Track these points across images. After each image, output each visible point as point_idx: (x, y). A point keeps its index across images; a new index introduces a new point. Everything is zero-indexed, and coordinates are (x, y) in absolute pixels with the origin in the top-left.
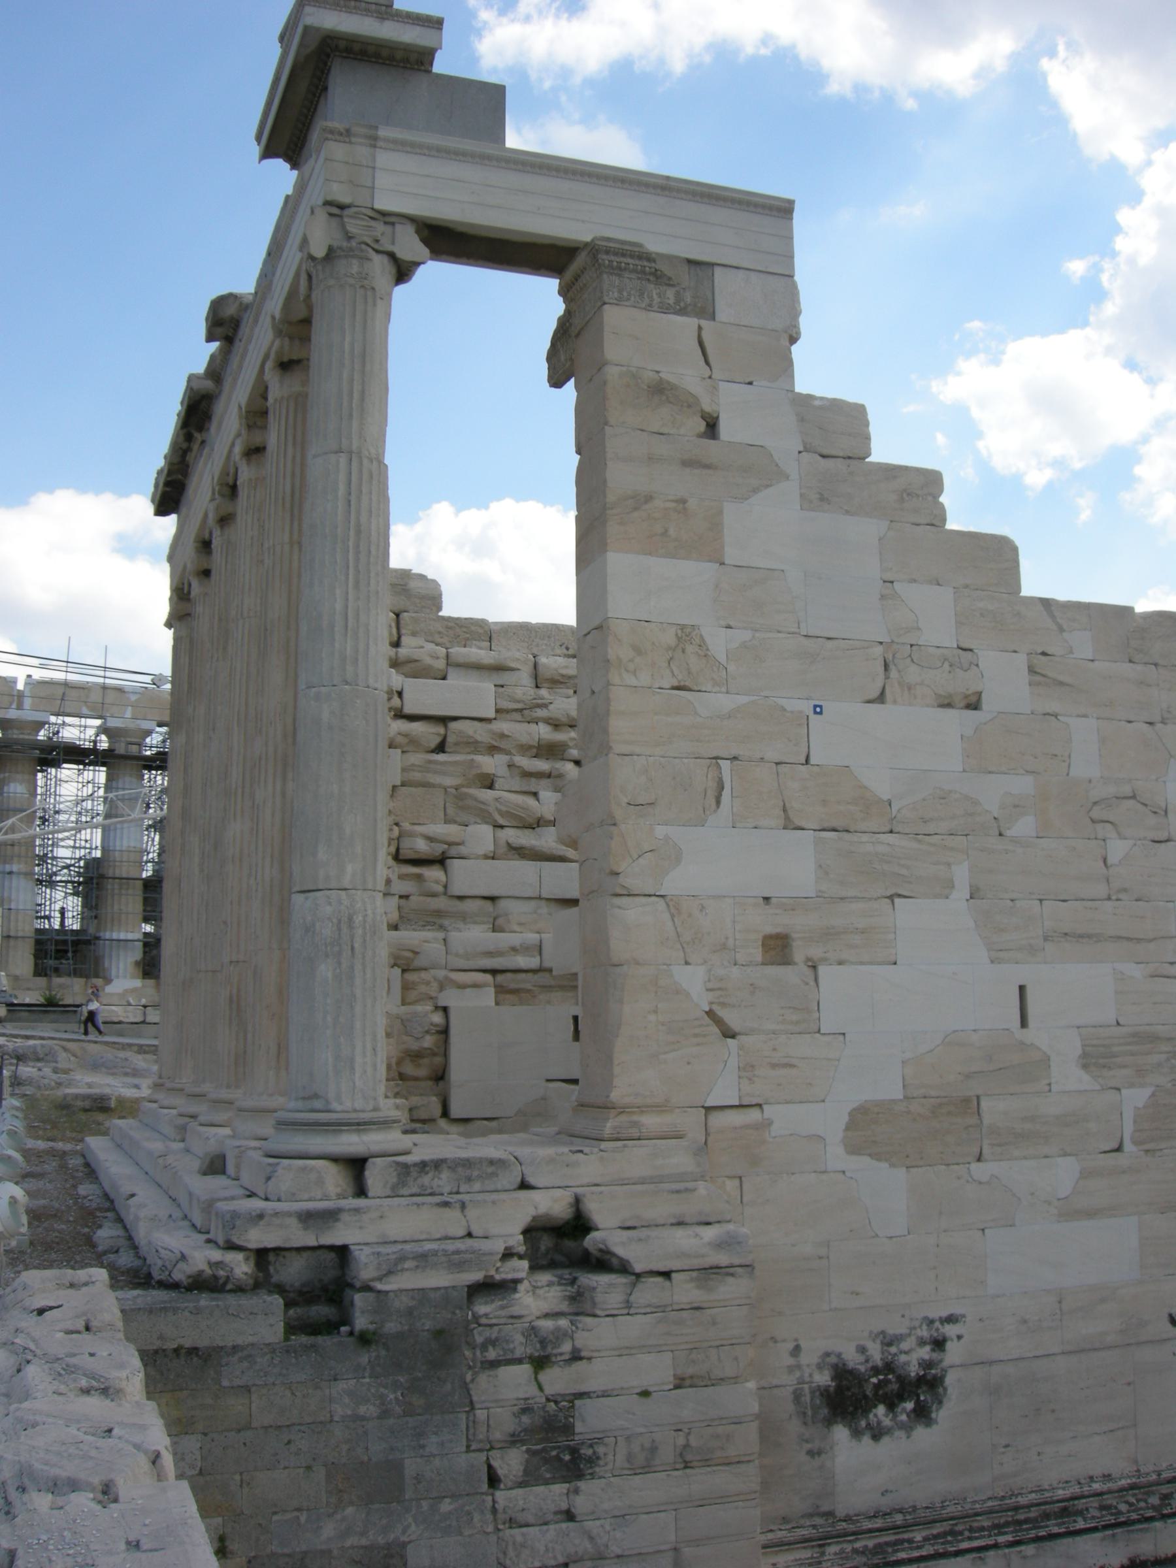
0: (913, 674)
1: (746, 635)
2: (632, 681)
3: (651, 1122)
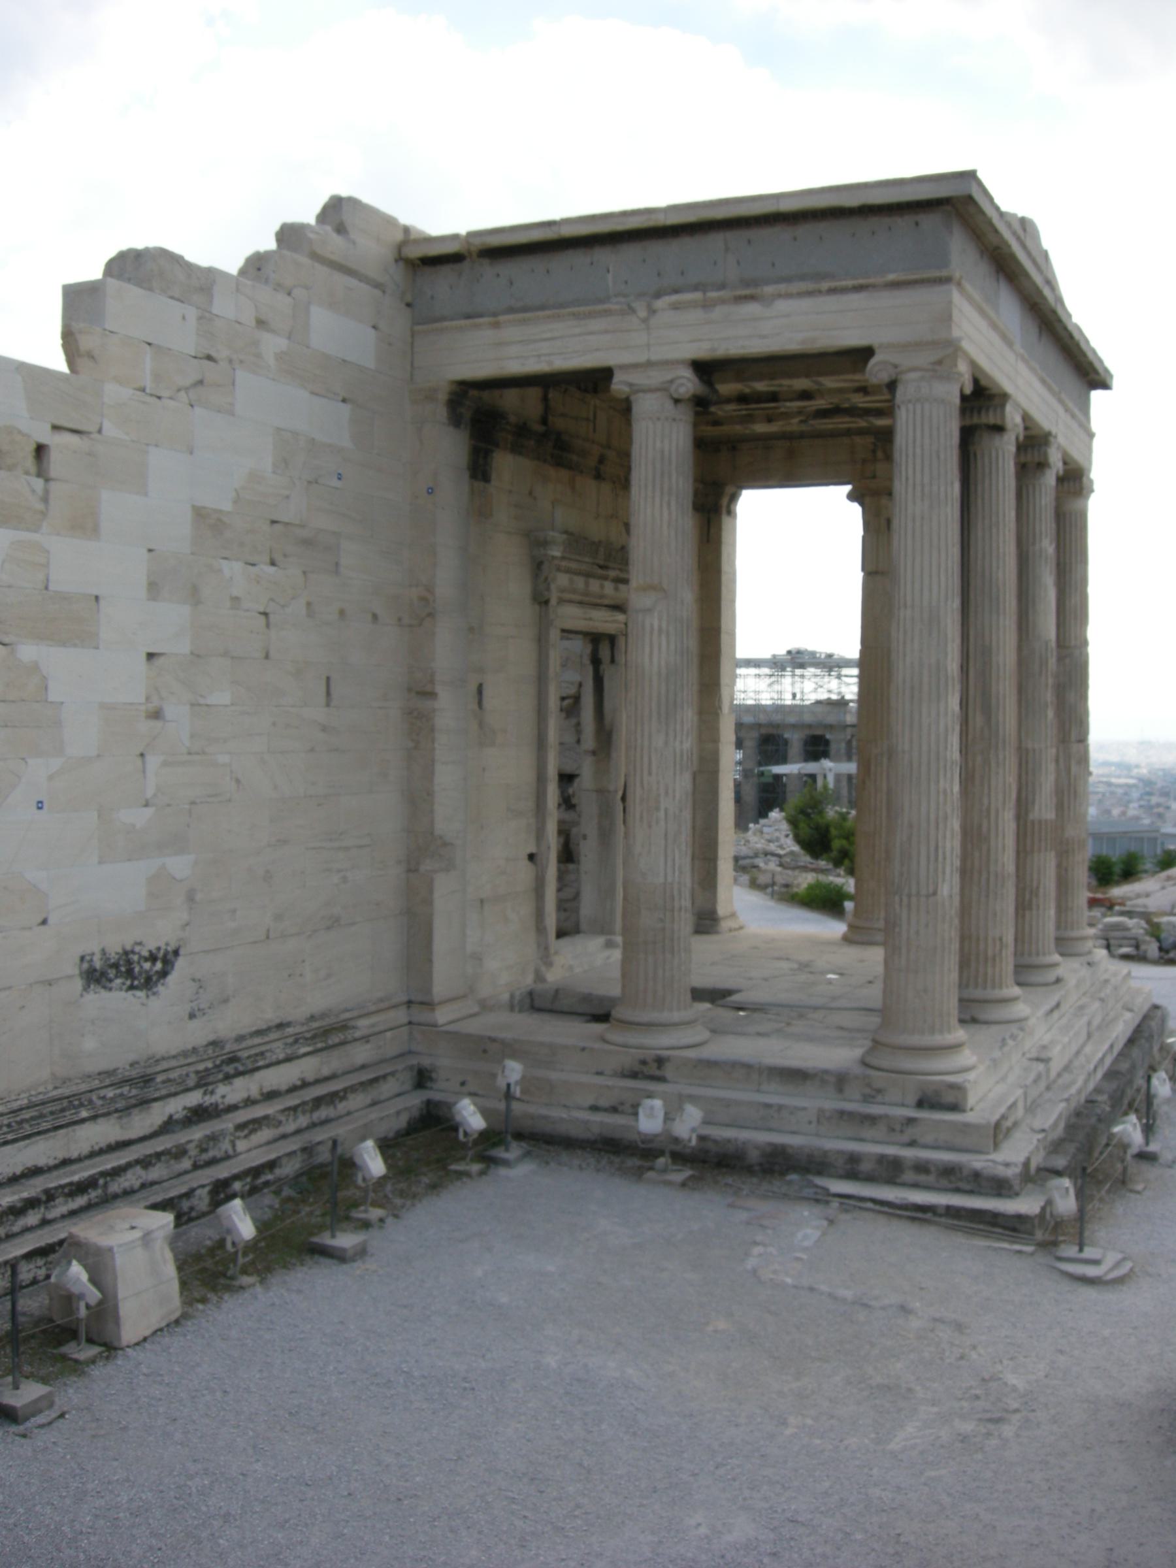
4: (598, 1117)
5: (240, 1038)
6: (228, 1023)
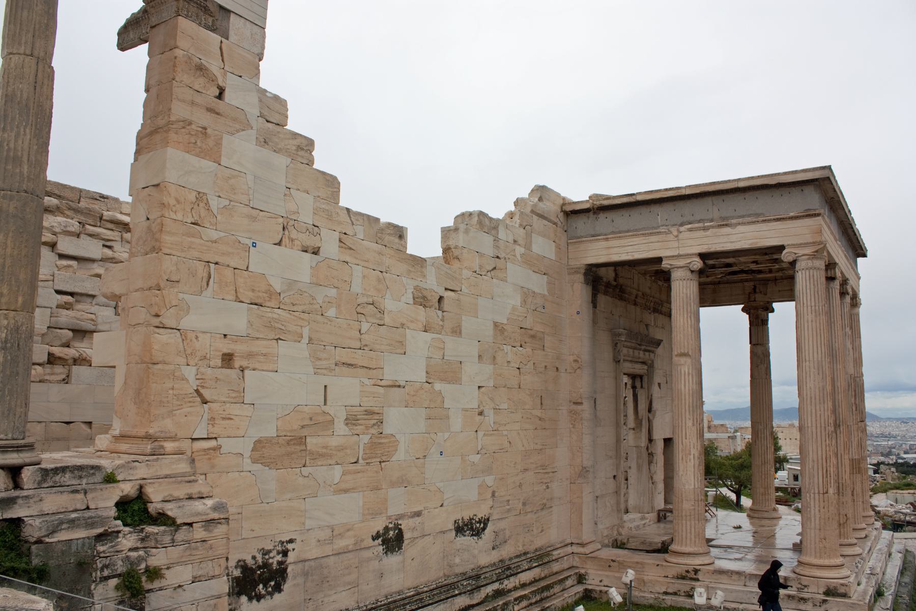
0: (294, 234)
1: (227, 203)
2: (175, 217)
3: (169, 446)
4: (668, 598)
5: (510, 559)
6: (507, 551)
